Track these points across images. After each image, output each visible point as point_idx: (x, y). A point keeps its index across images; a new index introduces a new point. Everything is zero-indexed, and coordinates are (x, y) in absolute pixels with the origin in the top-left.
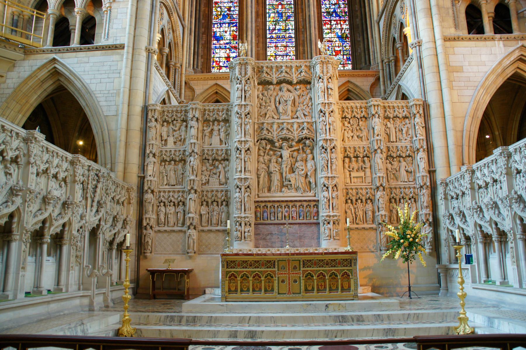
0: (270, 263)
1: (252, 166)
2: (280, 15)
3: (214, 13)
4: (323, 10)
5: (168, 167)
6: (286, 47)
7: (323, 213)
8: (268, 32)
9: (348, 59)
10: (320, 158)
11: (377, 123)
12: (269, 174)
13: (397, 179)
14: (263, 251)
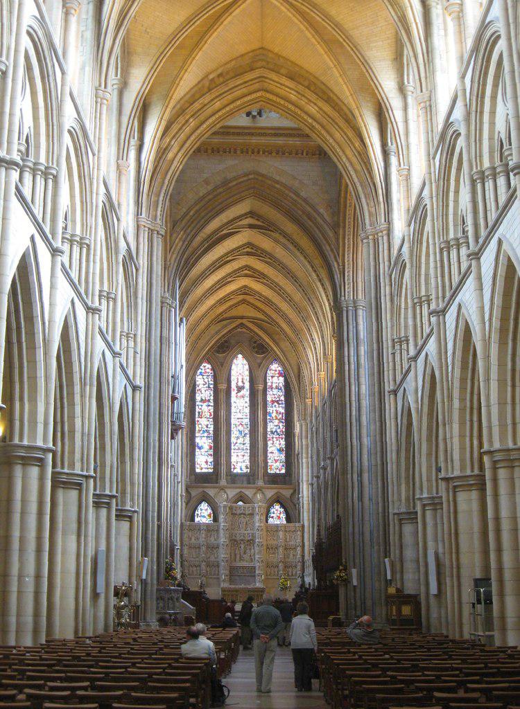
0: (237, 591)
1: (228, 552)
2: (240, 432)
3: (197, 429)
4: (269, 430)
5: (193, 551)
6: (243, 456)
7: (257, 572)
8: (232, 445)
9: (283, 466)
10: (257, 549)
11: (281, 534)
12: (235, 555)
13: (288, 558)
14: (233, 586)
